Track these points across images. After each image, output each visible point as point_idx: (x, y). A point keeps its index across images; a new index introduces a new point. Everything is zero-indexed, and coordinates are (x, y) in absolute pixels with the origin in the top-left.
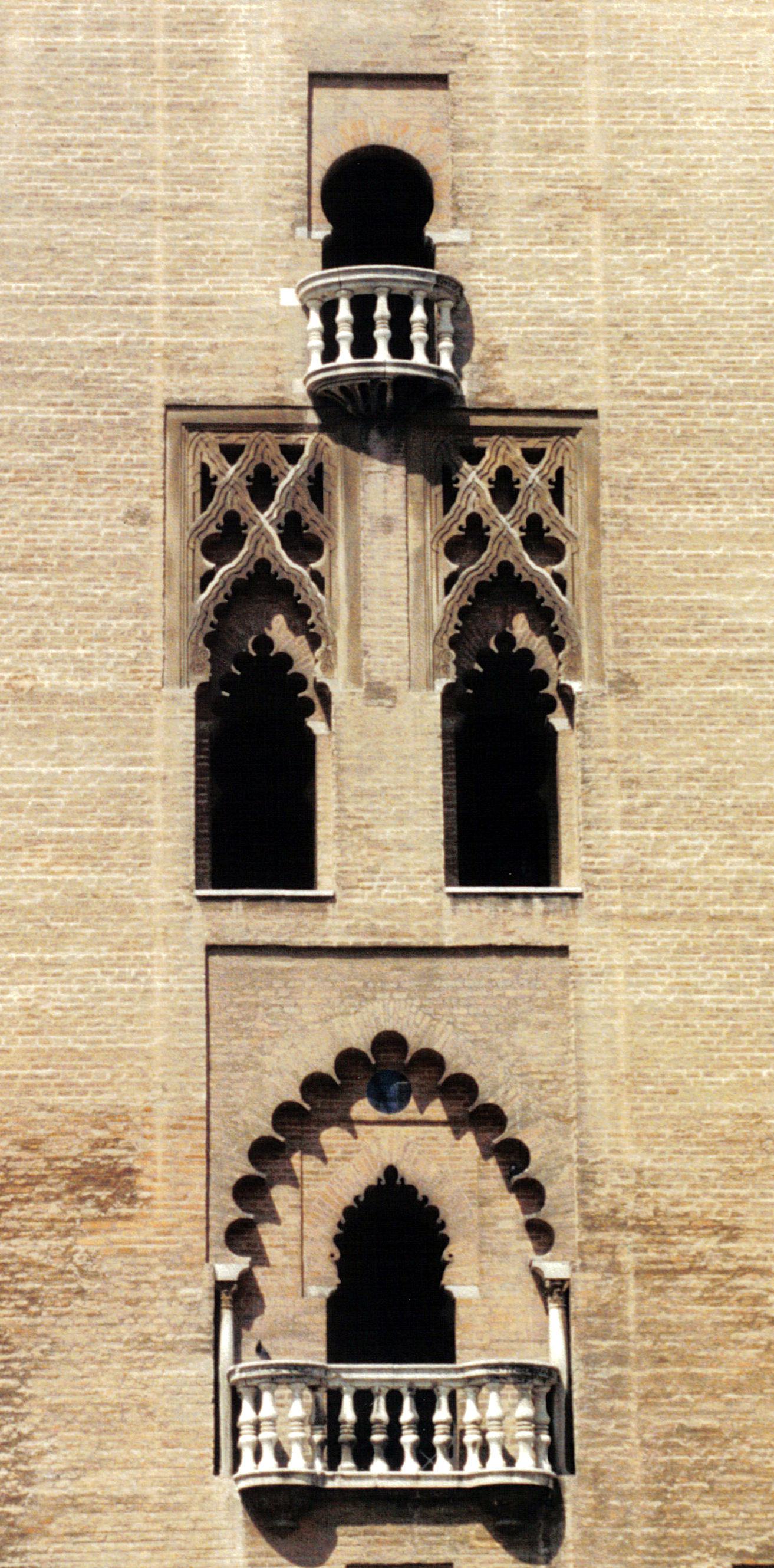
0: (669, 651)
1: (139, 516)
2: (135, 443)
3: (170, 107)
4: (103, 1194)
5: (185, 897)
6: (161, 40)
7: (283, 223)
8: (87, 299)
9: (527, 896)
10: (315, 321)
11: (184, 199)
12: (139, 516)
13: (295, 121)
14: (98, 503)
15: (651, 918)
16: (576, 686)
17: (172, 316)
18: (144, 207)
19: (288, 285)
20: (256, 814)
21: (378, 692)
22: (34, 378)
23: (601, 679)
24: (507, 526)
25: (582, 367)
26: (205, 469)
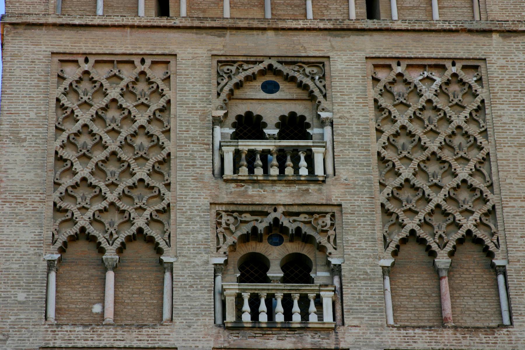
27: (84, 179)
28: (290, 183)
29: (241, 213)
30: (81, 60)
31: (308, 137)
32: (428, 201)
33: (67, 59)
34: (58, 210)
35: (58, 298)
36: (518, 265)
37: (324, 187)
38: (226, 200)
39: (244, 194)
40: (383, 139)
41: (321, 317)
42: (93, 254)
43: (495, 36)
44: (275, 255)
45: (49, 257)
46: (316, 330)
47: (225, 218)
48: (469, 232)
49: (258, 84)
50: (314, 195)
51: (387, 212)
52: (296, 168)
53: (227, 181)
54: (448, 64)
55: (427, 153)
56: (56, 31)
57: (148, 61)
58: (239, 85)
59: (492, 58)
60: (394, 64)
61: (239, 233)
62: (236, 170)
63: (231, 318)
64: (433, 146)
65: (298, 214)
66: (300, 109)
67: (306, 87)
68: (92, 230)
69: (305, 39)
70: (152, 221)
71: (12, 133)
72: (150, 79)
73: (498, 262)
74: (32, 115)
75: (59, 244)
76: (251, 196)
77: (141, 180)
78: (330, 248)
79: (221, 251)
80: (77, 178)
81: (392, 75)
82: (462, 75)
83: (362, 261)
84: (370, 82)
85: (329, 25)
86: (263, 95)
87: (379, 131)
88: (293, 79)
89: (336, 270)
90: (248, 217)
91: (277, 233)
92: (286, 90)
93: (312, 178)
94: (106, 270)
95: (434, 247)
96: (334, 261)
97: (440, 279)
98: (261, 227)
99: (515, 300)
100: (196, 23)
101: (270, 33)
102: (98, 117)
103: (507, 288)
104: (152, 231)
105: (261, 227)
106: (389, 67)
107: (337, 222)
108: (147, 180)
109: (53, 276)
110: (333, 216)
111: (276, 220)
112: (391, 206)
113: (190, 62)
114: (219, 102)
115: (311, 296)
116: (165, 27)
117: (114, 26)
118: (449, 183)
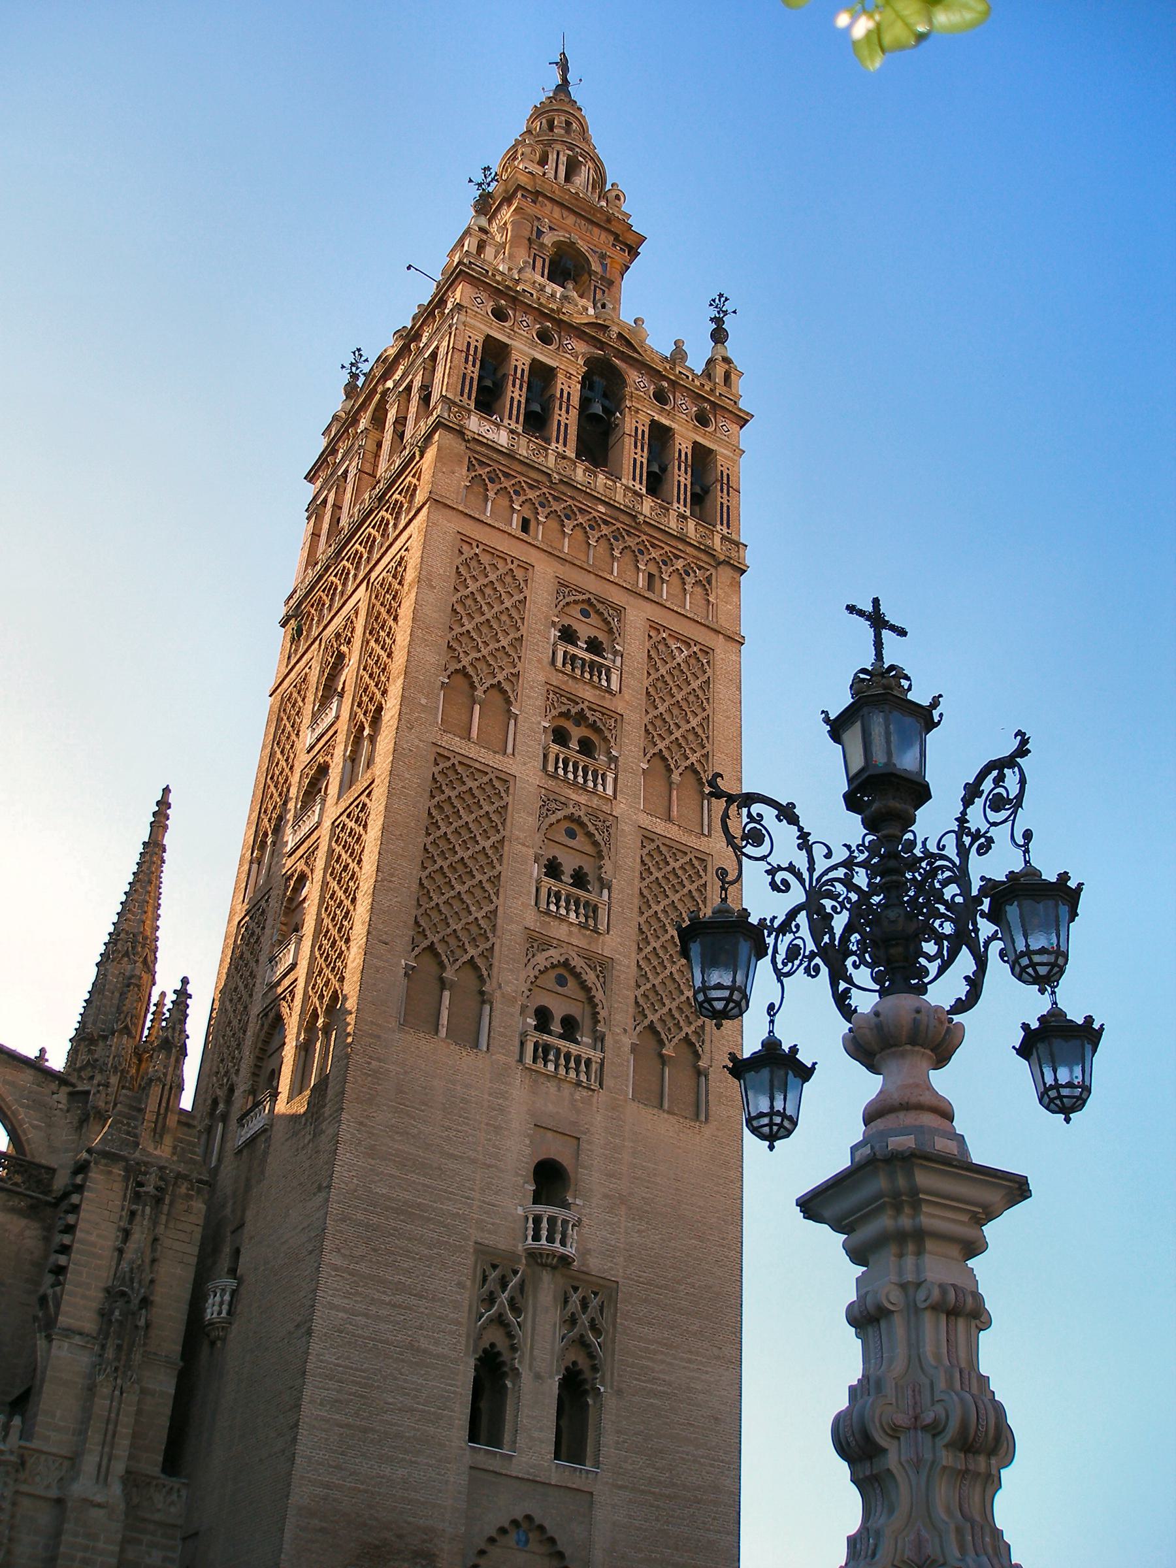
1: (460, 1285)
4: (424, 1563)
5: (463, 1445)
6: (486, 1096)
10: (531, 1224)
12: (460, 1285)
14: (448, 1276)
15: (620, 1487)
16: (602, 1390)
17: (480, 1207)
18: (473, 1161)
20: (487, 1418)
21: (538, 1376)
22: (429, 1219)
23: (612, 1388)
24: (584, 1319)
27: (468, 631)
28: (595, 687)
30: (474, 544)
33: (466, 540)
34: (450, 647)
40: (651, 679)
42: (466, 687)
44: (577, 733)
47: (551, 696)
51: (647, 731)
54: (692, 644)
56: (462, 516)
59: (718, 651)
62: (564, 665)
63: (551, 769)
65: (595, 711)
66: (602, 637)
68: (470, 670)
69: (613, 588)
72: (517, 576)
74: (441, 572)
80: (464, 629)
81: (659, 638)
82: (699, 654)
90: (565, 701)
92: (594, 619)
98: (573, 711)
101: (593, 576)
103: (709, 810)
105: (573, 711)
107: (619, 725)
112: (650, 727)
114: (556, 611)
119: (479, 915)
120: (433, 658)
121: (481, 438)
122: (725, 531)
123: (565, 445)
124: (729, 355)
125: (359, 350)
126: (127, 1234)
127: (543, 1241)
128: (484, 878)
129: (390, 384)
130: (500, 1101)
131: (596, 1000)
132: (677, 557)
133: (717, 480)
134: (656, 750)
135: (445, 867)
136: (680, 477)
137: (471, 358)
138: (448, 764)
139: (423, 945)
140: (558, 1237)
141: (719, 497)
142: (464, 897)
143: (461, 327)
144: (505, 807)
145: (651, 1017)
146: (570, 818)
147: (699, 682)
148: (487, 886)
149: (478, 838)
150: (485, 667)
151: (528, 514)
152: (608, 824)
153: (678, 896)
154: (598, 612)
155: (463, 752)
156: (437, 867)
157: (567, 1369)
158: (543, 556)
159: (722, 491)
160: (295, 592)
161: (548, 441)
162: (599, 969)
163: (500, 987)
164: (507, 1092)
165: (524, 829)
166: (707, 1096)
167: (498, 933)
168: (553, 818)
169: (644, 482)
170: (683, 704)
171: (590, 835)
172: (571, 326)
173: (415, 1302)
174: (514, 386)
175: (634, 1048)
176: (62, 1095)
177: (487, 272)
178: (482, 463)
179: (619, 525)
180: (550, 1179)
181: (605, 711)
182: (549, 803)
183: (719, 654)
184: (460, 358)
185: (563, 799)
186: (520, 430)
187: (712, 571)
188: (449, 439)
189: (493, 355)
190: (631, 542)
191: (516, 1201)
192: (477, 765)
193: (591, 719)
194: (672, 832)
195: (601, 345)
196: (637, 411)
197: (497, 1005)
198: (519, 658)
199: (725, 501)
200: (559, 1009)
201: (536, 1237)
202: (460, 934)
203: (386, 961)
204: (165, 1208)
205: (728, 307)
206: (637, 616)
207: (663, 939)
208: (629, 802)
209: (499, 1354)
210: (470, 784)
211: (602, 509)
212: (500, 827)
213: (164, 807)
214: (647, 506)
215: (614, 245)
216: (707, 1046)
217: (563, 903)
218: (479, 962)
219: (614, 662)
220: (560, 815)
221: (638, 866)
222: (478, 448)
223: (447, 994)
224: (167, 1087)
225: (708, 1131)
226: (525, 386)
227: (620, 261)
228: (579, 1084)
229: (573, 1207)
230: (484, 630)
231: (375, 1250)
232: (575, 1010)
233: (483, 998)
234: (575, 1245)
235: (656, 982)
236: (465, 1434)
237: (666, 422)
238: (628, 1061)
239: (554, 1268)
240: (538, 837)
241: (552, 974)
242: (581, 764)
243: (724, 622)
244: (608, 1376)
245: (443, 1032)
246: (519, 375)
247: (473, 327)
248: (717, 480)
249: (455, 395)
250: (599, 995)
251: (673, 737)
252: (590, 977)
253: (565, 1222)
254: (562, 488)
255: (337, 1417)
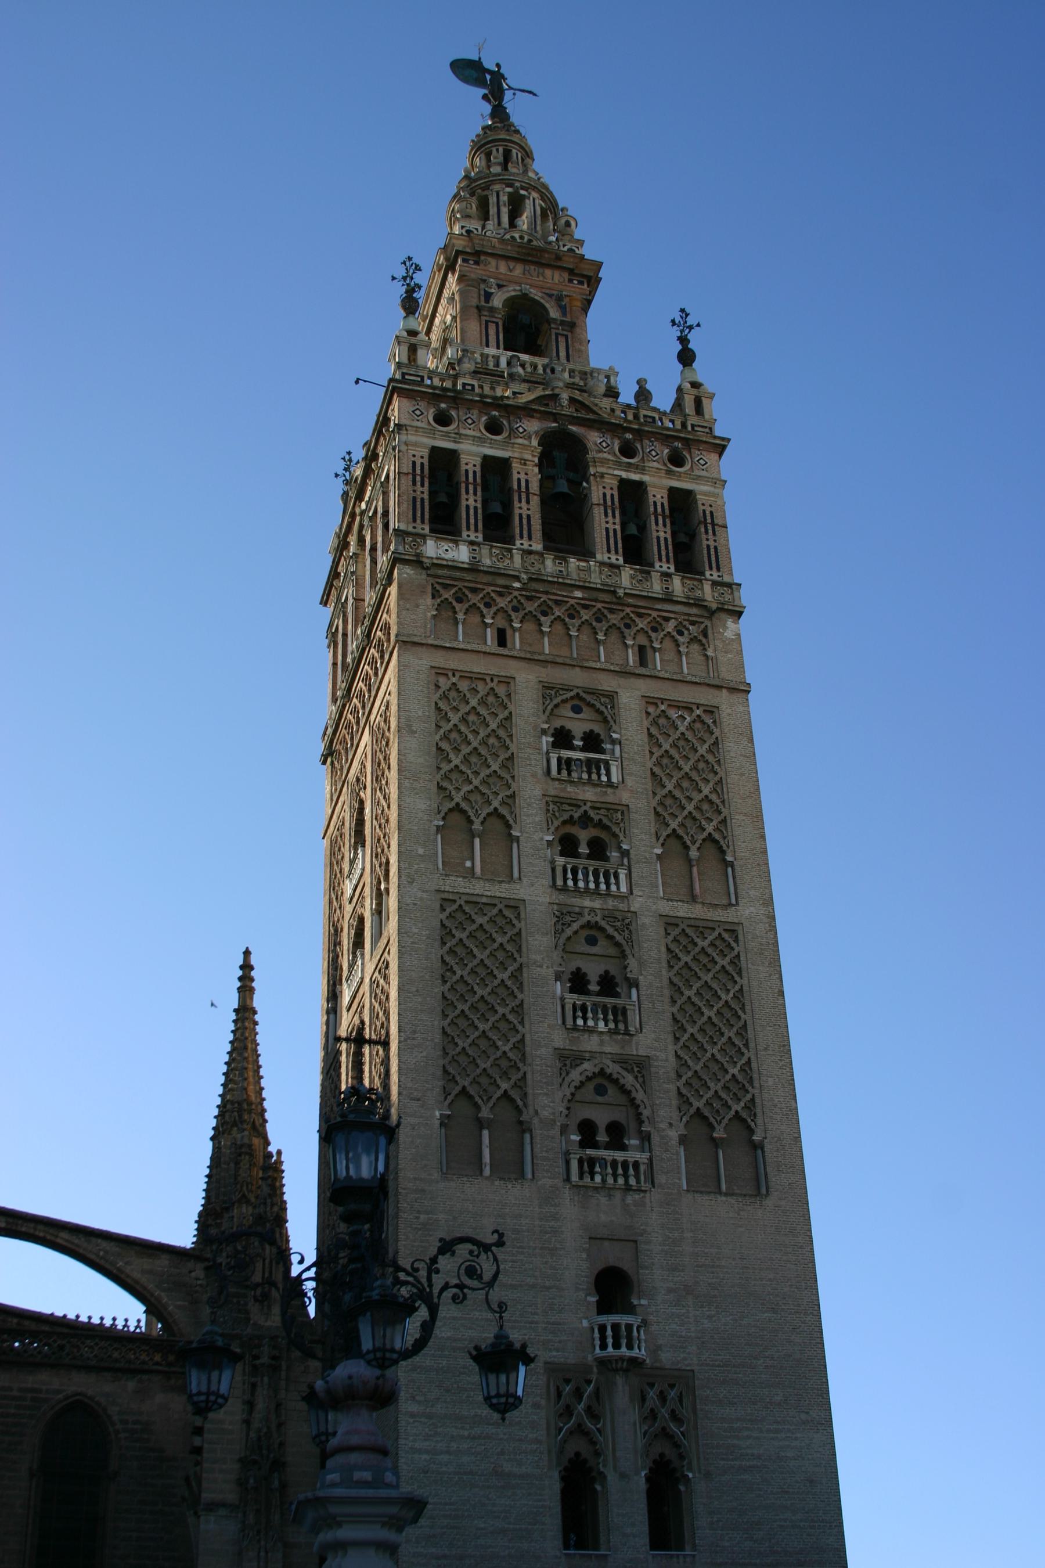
0: (722, 1463)
2: (534, 1378)
3: (541, 1248)
5: (558, 1554)
6: (537, 1222)
7: (582, 1294)
8: (515, 1321)
9: (678, 1556)
10: (597, 1335)
11: (547, 1284)
13: (584, 1256)
16: (690, 1475)
19: (587, 1318)
21: (623, 1476)
23: (700, 1472)
24: (664, 1412)
25: (689, 1353)
26: (558, 1388)
28: (595, 785)
29: (562, 803)
30: (450, 674)
31: (603, 751)
32: (684, 808)
33: (440, 672)
34: (440, 788)
35: (443, 853)
36: (741, 862)
37: (617, 791)
38: (553, 793)
39: (564, 790)
40: (654, 759)
41: (618, 888)
43: (724, 691)
45: (436, 823)
46: (615, 897)
48: (710, 834)
49: (569, 705)
50: (611, 797)
51: (657, 814)
52: (599, 775)
53: (553, 779)
54: (694, 707)
55: (682, 773)
57: (496, 680)
58: (556, 706)
59: (723, 707)
60: (659, 704)
61: (562, 819)
62: (559, 772)
63: (560, 882)
64: (687, 768)
65: (599, 809)
66: (597, 728)
67: (602, 713)
68: (464, 805)
69: (602, 676)
70: (503, 803)
71: (408, 726)
72: (498, 695)
73: (729, 858)
74: (420, 713)
75: (442, 814)
76: (569, 792)
77: (495, 772)
78: (622, 838)
79: (551, 831)
80: (452, 765)
81: (658, 711)
83: (643, 849)
84: (644, 715)
85: (617, 669)
86: (572, 714)
87: (651, 753)
88: (593, 706)
89: (625, 854)
90: (567, 808)
91: (585, 821)
93: (610, 784)
94: (473, 836)
95: (689, 843)
96: (625, 847)
97: (691, 866)
98: (576, 816)
99: (740, 887)
100: (528, 656)
101: (578, 669)
102: (464, 720)
103: (734, 878)
104: (504, 811)
106: (656, 704)
107: (626, 818)
108: (499, 772)
109: (439, 836)
110: (623, 812)
111: (586, 812)
112: (659, 809)
113: (524, 685)
114: (544, 718)
115: (612, 871)
116: (507, 656)
117: (472, 651)
118: (697, 797)
119: (507, 1048)
120: (423, 804)
121: (440, 562)
122: (715, 574)
123: (530, 538)
124: (700, 379)
125: (349, 453)
126: (250, 1405)
127: (610, 1349)
128: (506, 1010)
129: (363, 506)
130: (552, 1223)
131: (638, 1102)
132: (667, 619)
133: (700, 522)
134: (669, 831)
135: (466, 1009)
136: (660, 532)
137: (418, 478)
138: (455, 907)
139: (454, 1093)
140: (624, 1342)
141: (705, 540)
142: (490, 1034)
143: (404, 448)
144: (519, 934)
145: (697, 1104)
146: (588, 925)
147: (706, 746)
148: (511, 1017)
149: (496, 972)
150: (479, 797)
151: (501, 623)
152: (627, 921)
153: (711, 975)
154: (589, 704)
155: (468, 891)
156: (458, 1012)
157: (655, 1462)
158: (522, 664)
159: (707, 532)
160: (326, 728)
161: (511, 541)
162: (636, 1069)
163: (536, 1112)
164: (557, 1213)
165: (540, 950)
166: (765, 1168)
167: (529, 1060)
168: (569, 932)
169: (620, 551)
170: (694, 775)
171: (610, 938)
172: (518, 408)
173: (494, 1431)
174: (467, 493)
175: (683, 1140)
176: (199, 1272)
177: (422, 377)
178: (446, 587)
179: (599, 605)
180: (613, 1288)
181: (609, 806)
182: (563, 917)
183: (725, 710)
184: (407, 481)
185: (577, 910)
186: (480, 539)
187: (707, 622)
188: (408, 570)
189: (442, 465)
190: (614, 619)
191: (580, 1315)
192: (484, 900)
193: (596, 818)
194: (697, 911)
195: (555, 417)
196: (602, 476)
197: (537, 1132)
198: (513, 777)
199: (711, 543)
200: (602, 1118)
201: (604, 1346)
202: (490, 1071)
203: (421, 1117)
204: (283, 1374)
205: (690, 321)
206: (630, 698)
207: (700, 1023)
208: (646, 892)
209: (585, 1461)
210: (480, 920)
211: (578, 594)
212: (516, 955)
213: (247, 971)
214: (626, 578)
215: (570, 281)
216: (759, 1120)
217: (590, 1015)
218: (514, 1094)
219: (613, 751)
220: (575, 926)
221: (664, 956)
222: (440, 572)
223: (486, 1133)
224: (267, 1262)
225: (769, 1202)
226: (479, 489)
227: (579, 297)
228: (628, 1188)
229: (638, 1310)
230: (474, 759)
231: (448, 1391)
232: (619, 1115)
233: (523, 1128)
234: (643, 1345)
235: (698, 1068)
236: (559, 1543)
237: (635, 477)
238: (678, 1154)
239: (626, 1371)
240: (556, 956)
241: (591, 1086)
242: (591, 869)
243: (726, 674)
244: (695, 1462)
245: (487, 1172)
246: (471, 479)
247: (416, 444)
248: (700, 522)
249: (408, 523)
250: (639, 1096)
251: (686, 812)
252: (628, 1080)
253: (629, 1327)
254: (535, 585)
255: (434, 1550)
